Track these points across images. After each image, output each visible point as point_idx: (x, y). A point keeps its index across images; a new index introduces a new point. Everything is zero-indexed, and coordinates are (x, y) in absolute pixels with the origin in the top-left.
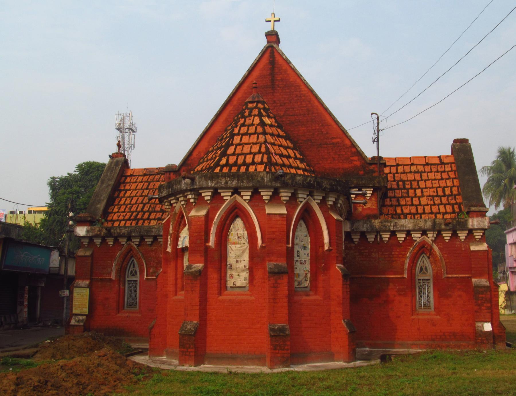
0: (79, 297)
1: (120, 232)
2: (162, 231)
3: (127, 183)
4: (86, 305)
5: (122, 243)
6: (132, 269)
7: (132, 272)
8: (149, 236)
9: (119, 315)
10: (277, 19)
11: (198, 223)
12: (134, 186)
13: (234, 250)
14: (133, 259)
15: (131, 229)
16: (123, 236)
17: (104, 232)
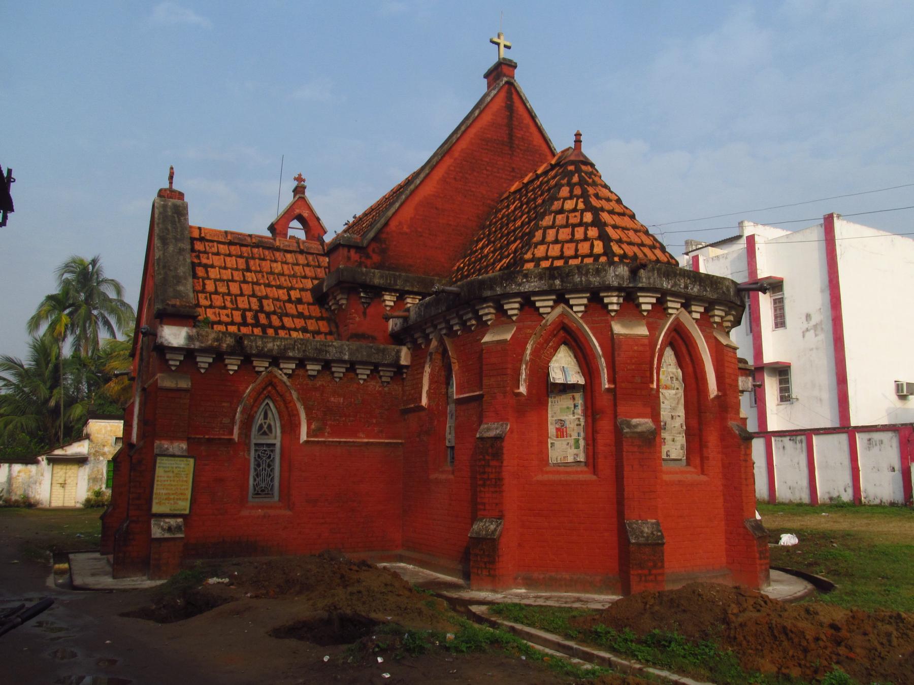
0: (168, 477)
1: (263, 348)
2: (347, 353)
3: (200, 252)
4: (185, 494)
5: (257, 369)
6: (263, 421)
7: (261, 427)
8: (315, 360)
9: (245, 513)
10: (508, 44)
11: (636, 348)
12: (217, 261)
13: (668, 398)
14: (267, 401)
15: (286, 342)
16: (261, 355)
17: (228, 342)
